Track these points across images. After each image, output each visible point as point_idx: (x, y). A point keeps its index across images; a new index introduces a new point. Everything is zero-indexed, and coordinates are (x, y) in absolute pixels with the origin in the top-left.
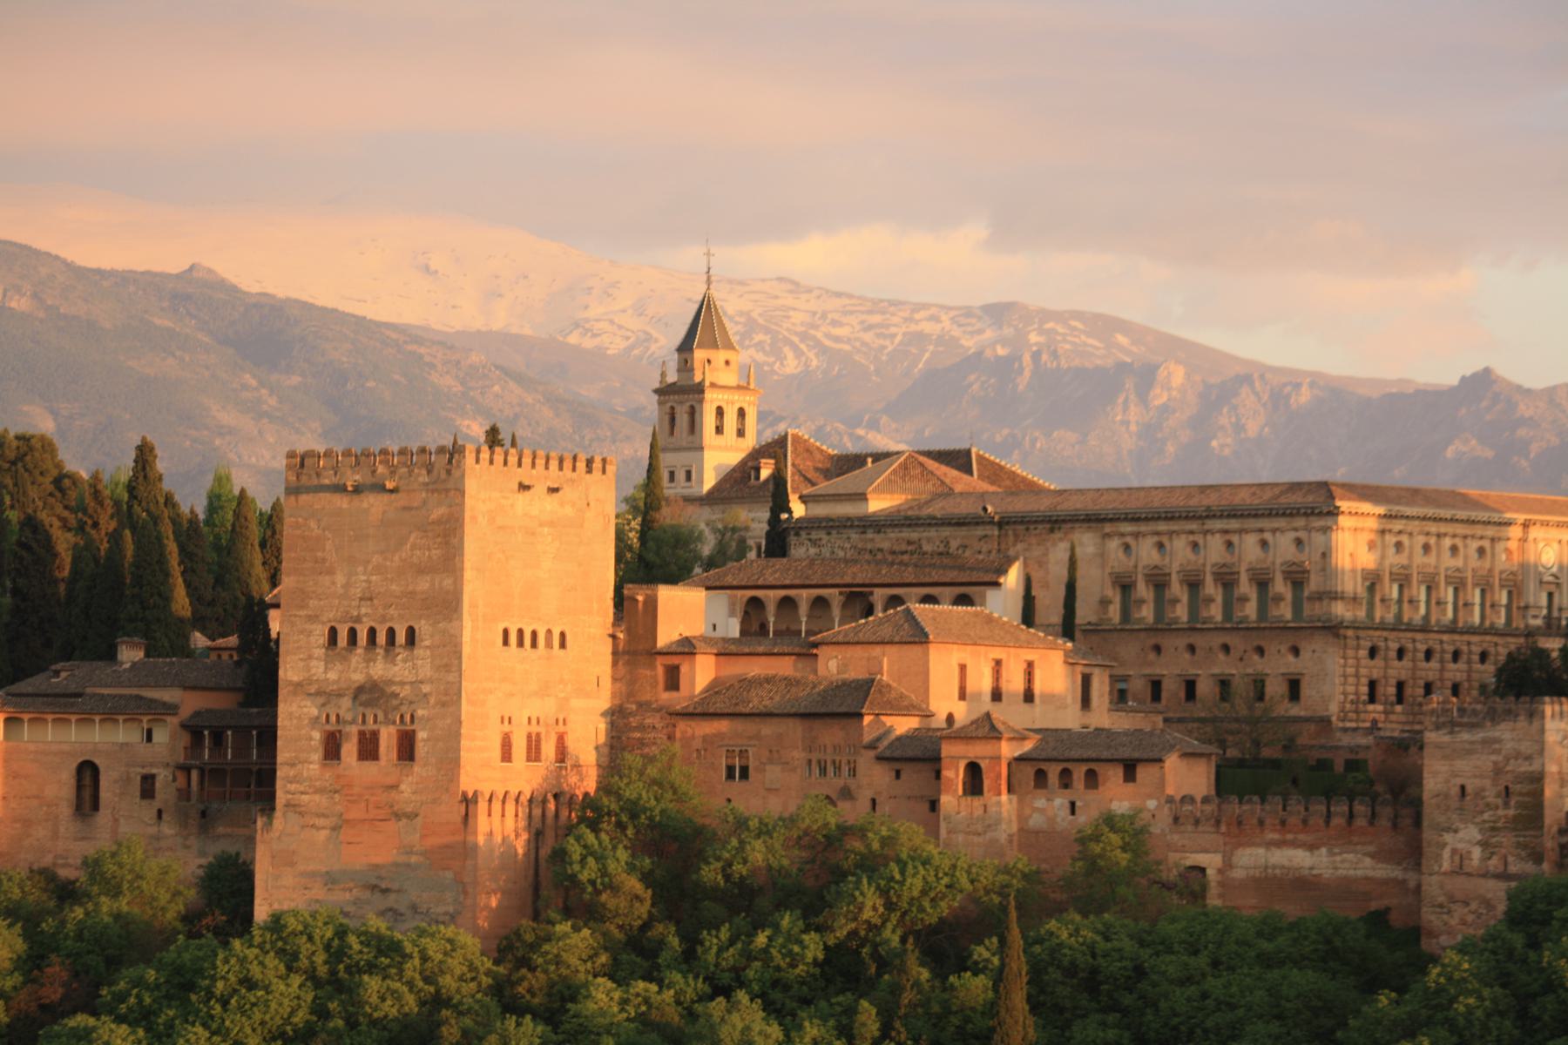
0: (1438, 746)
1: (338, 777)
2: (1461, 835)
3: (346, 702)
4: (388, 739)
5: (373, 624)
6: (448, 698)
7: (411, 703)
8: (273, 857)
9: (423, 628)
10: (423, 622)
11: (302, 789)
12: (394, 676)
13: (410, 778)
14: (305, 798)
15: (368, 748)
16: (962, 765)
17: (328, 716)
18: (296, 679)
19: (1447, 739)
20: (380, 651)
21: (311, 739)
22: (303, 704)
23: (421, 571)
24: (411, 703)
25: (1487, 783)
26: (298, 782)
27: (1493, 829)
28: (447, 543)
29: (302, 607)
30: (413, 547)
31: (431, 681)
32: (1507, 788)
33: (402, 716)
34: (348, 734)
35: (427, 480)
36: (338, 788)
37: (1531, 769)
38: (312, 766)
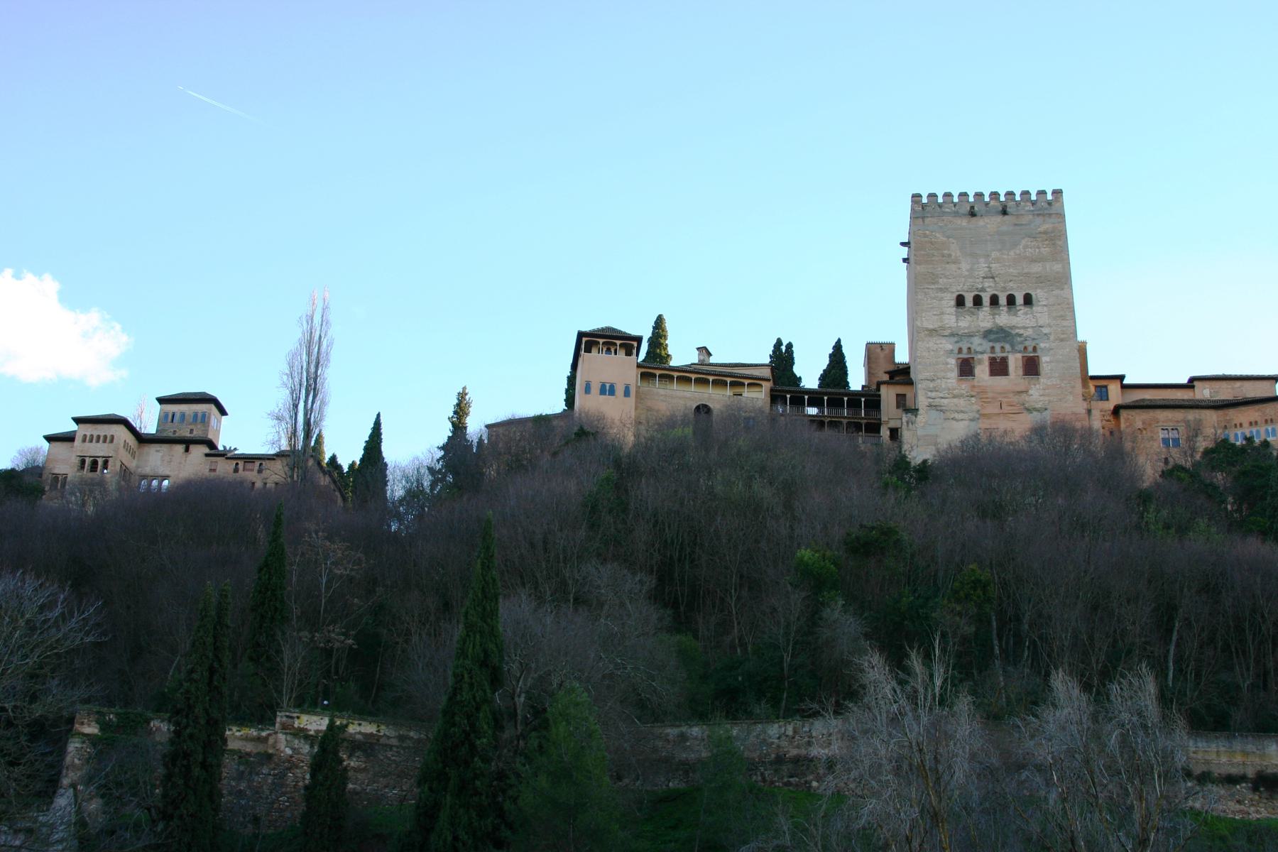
1: (973, 387)
4: (1015, 362)
5: (996, 293)
7: (1034, 339)
9: (1038, 294)
10: (1039, 291)
11: (942, 395)
13: (1037, 386)
14: (945, 401)
15: (999, 368)
18: (931, 327)
20: (1005, 309)
21: (947, 364)
22: (938, 342)
23: (1033, 260)
26: (937, 391)
29: (933, 283)
30: (1026, 247)
31: (1049, 326)
33: (1025, 348)
35: (1032, 208)
36: (973, 393)
38: (949, 381)
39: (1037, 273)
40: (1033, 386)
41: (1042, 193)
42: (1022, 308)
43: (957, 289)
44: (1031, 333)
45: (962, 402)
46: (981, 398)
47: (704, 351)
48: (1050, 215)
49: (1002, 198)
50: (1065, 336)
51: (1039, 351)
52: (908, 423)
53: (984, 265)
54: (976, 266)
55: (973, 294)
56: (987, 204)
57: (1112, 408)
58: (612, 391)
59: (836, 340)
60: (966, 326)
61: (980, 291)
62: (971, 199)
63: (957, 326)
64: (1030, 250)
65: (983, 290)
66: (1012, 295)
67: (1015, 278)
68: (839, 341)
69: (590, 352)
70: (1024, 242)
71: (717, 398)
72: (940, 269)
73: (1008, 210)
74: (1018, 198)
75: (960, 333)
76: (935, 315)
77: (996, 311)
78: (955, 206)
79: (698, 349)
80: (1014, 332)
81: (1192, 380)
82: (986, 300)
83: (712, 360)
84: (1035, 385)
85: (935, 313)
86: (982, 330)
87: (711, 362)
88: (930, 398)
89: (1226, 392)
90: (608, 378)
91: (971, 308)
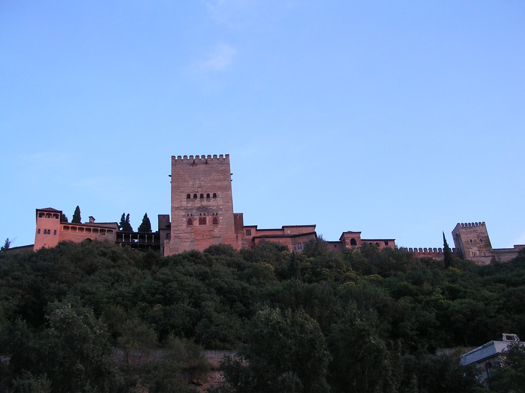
0: (464, 232)
1: (192, 229)
2: (473, 249)
3: (194, 211)
4: (209, 219)
6: (228, 209)
7: (216, 210)
8: (171, 250)
9: (219, 193)
10: (219, 192)
11: (180, 232)
12: (210, 204)
13: (217, 228)
15: (203, 221)
16: (350, 239)
17: (188, 215)
18: (177, 206)
19: (465, 231)
21: (183, 220)
23: (217, 181)
24: (216, 210)
25: (477, 239)
26: (178, 231)
27: (480, 247)
28: (225, 175)
29: (178, 190)
31: (223, 205)
32: (481, 239)
33: (213, 214)
34: (195, 219)
35: (217, 161)
36: (193, 232)
37: (485, 235)
38: (183, 227)
39: (218, 186)
40: (216, 228)
41: (221, 156)
42: (212, 199)
43: (188, 191)
44: (215, 208)
45: (188, 235)
46: (195, 233)
47: (92, 218)
48: (224, 163)
49: (206, 158)
50: (228, 209)
51: (218, 215)
52: (166, 243)
53: (198, 183)
54: (195, 183)
55: (193, 194)
56: (200, 159)
57: (252, 238)
58: (49, 233)
59: (145, 214)
60: (191, 205)
61: (196, 192)
62: (194, 158)
63: (187, 206)
64: (216, 177)
65: (197, 192)
66: (209, 194)
67: (210, 188)
68: (146, 213)
69: (41, 217)
70: (214, 174)
71: (93, 236)
72: (181, 184)
73: (208, 162)
74: (212, 157)
75: (188, 209)
76: (178, 202)
77: (202, 200)
78: (188, 160)
79: (89, 217)
80: (209, 208)
81: (283, 227)
82: (199, 196)
83: (95, 222)
84: (216, 228)
85: (179, 201)
86: (196, 207)
87: (95, 222)
88: (176, 234)
89: (296, 232)
90: (48, 228)
91: (192, 199)
